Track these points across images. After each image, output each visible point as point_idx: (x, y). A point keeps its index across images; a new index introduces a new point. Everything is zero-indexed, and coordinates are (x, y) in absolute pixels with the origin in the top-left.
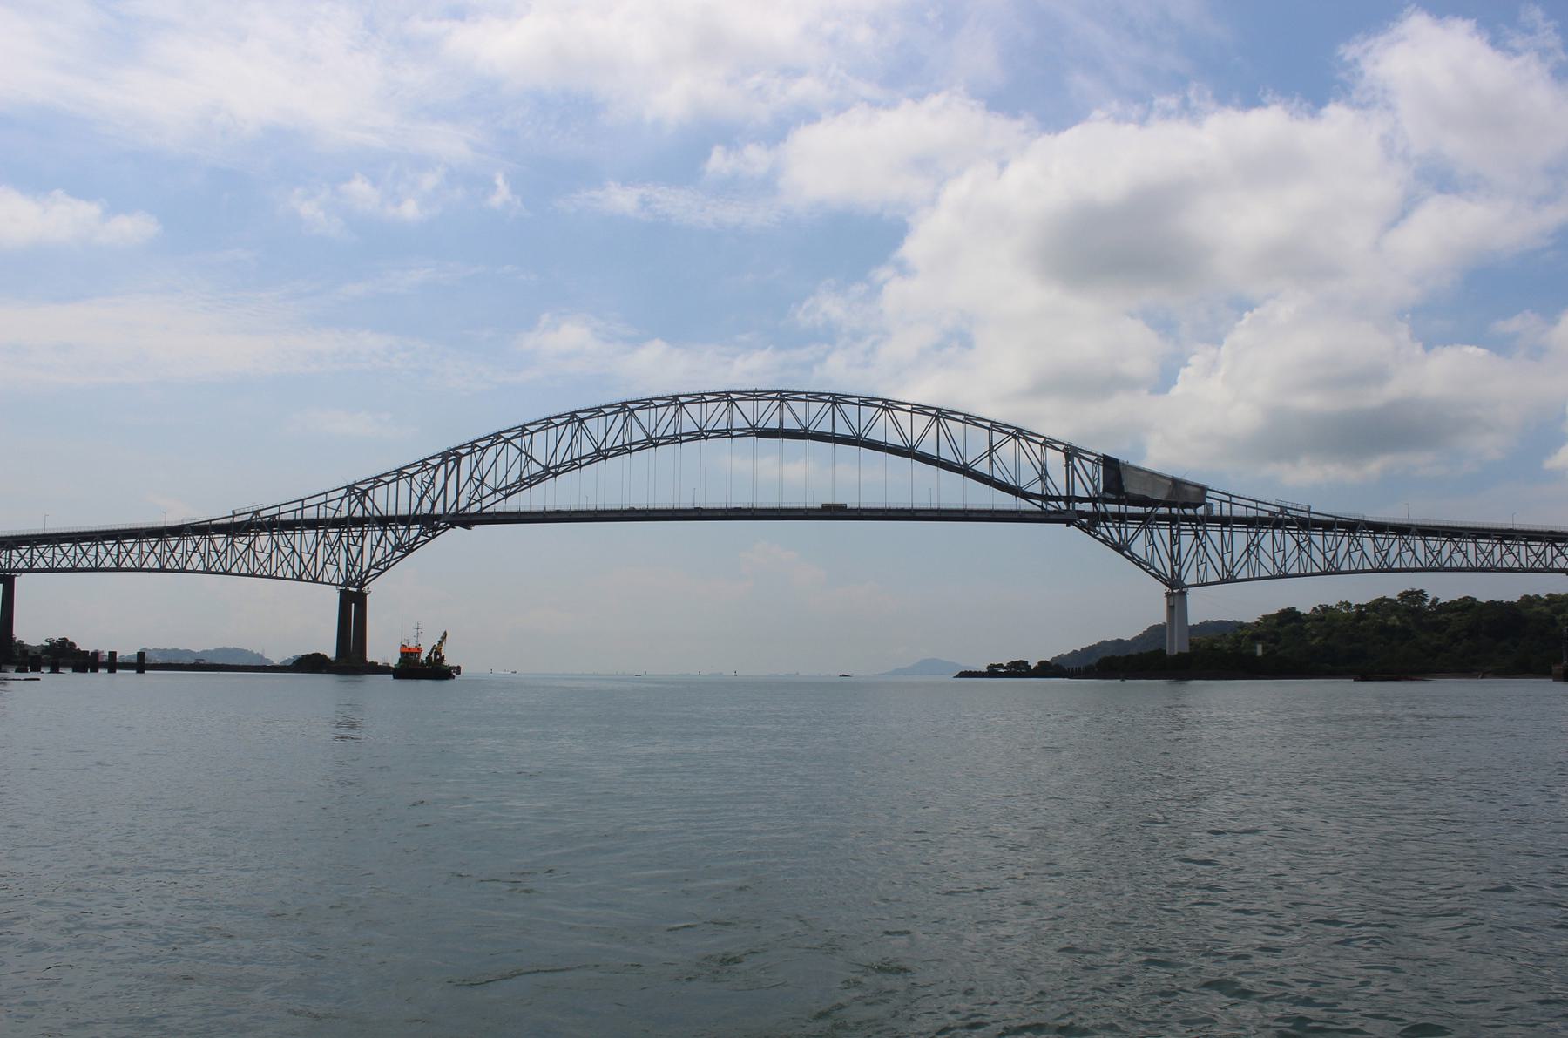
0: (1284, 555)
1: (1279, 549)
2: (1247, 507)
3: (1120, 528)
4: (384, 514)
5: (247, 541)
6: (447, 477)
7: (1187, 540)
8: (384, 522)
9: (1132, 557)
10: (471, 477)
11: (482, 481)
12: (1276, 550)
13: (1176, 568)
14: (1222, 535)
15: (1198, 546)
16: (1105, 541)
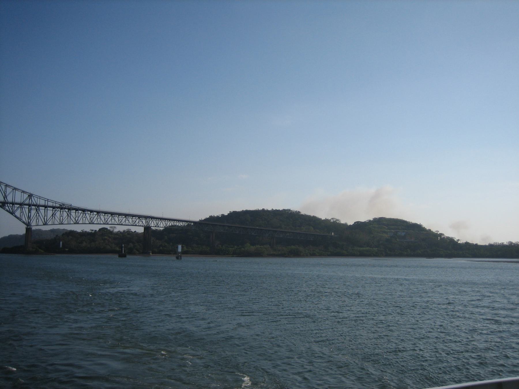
0: (63, 219)
1: (62, 216)
2: (53, 203)
3: (12, 207)
7: (33, 212)
9: (16, 216)
12: (76, 217)
13: (29, 220)
14: (45, 211)
15: (37, 214)
16: (7, 211)
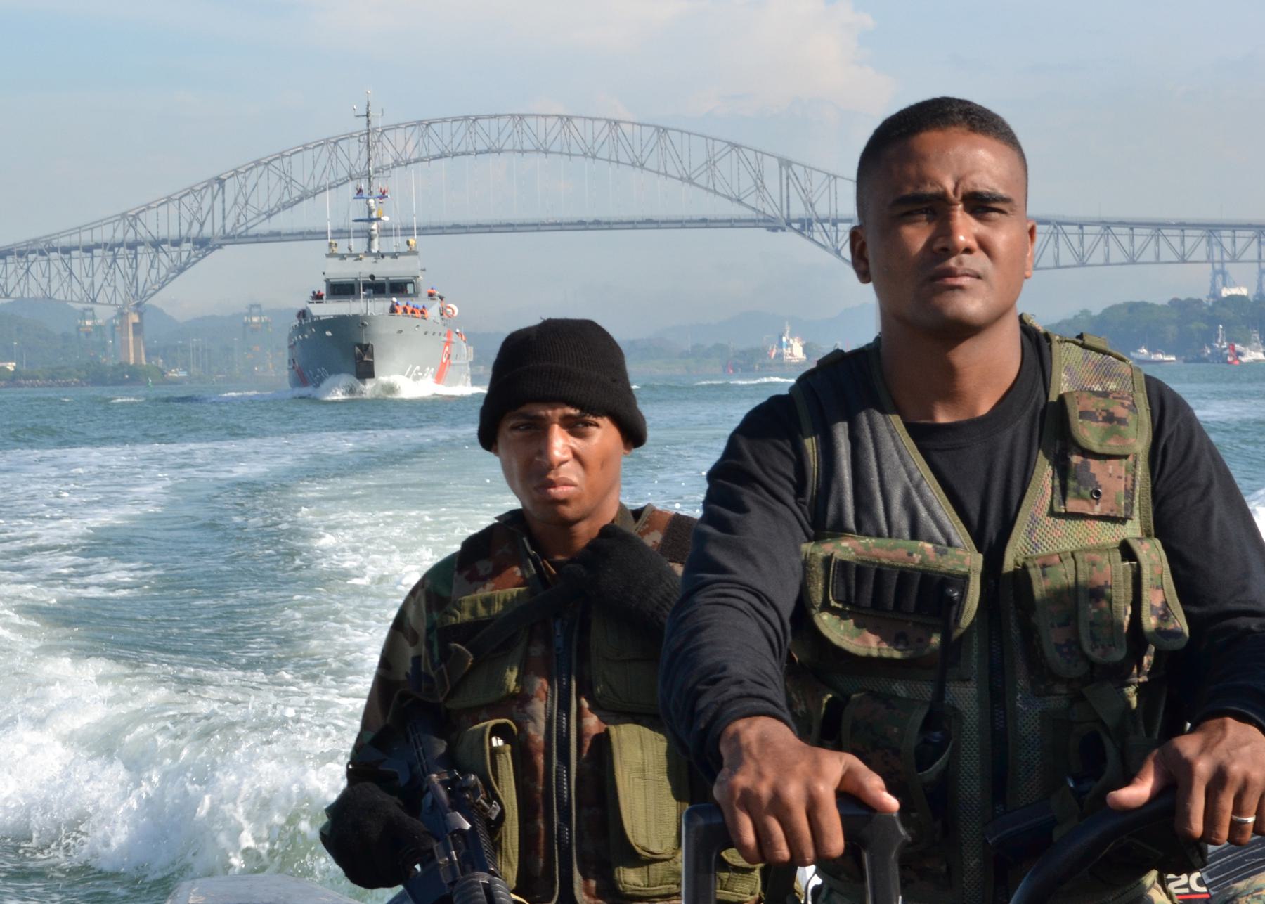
4: (155, 235)
5: (26, 267)
6: (214, 198)
8: (156, 244)
10: (235, 203)
11: (247, 203)
